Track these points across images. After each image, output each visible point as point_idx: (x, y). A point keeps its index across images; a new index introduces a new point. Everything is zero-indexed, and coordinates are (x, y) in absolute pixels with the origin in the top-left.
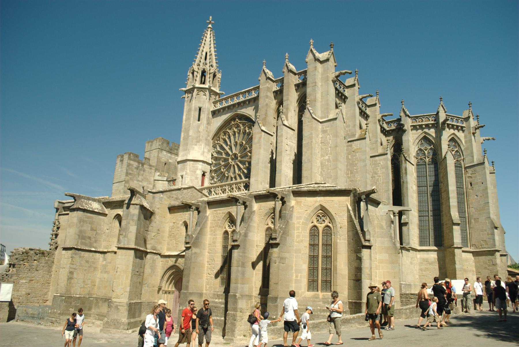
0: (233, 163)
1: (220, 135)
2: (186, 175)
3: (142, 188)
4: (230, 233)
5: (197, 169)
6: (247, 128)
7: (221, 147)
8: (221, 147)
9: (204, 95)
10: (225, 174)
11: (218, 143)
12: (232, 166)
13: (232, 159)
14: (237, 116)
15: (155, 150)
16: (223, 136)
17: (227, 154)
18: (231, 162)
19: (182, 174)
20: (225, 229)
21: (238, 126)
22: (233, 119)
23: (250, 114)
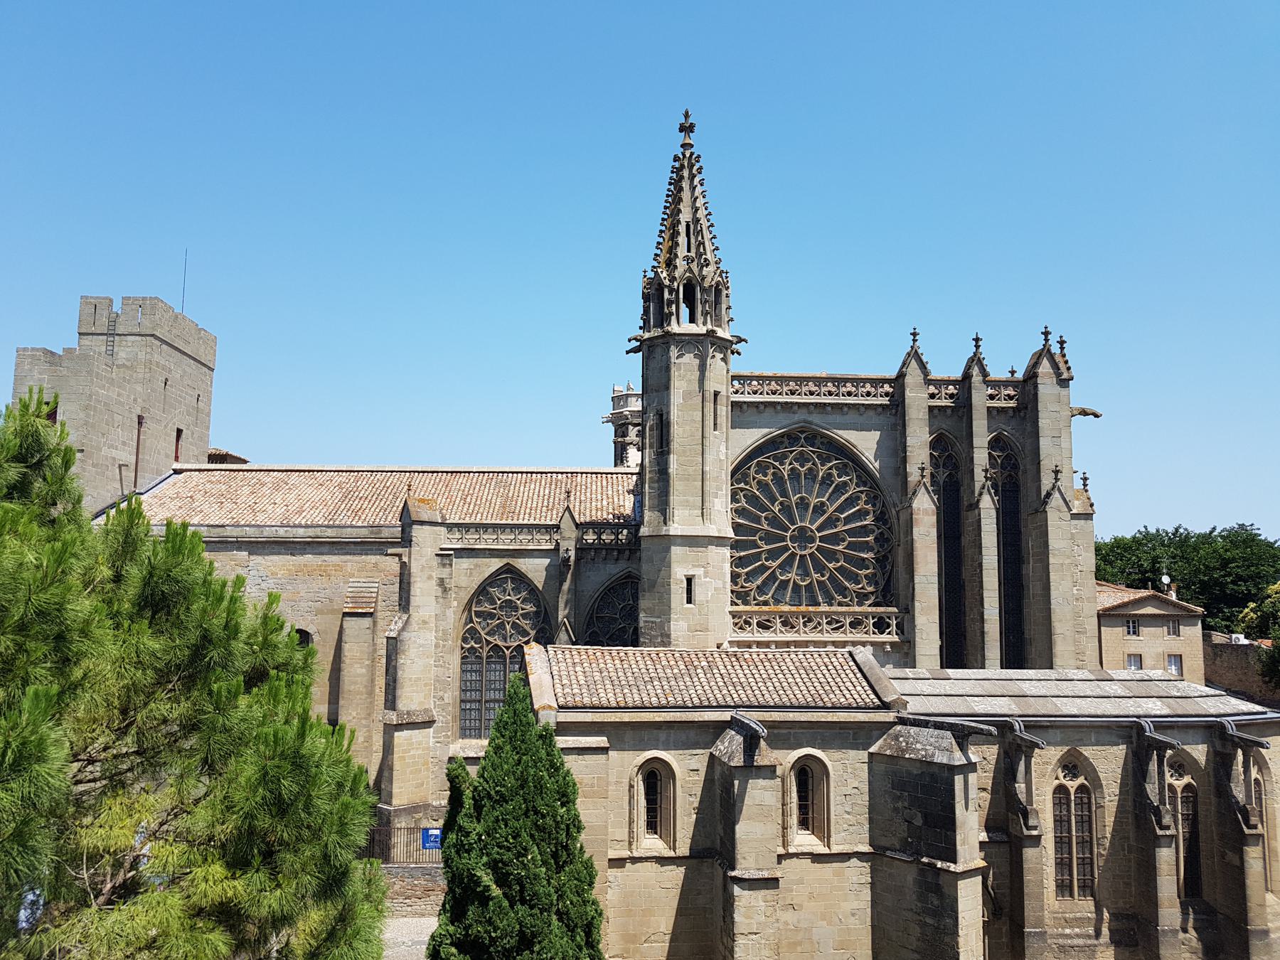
0: (799, 552)
1: (749, 468)
2: (705, 577)
3: (118, 470)
4: (1072, 791)
5: (723, 561)
6: (835, 472)
7: (752, 499)
8: (752, 499)
9: (722, 359)
10: (778, 573)
11: (742, 490)
12: (798, 557)
13: (793, 539)
14: (802, 432)
15: (138, 338)
16: (756, 472)
17: (773, 521)
18: (794, 547)
19: (691, 573)
20: (1057, 782)
21: (802, 458)
22: (790, 438)
23: (852, 441)
